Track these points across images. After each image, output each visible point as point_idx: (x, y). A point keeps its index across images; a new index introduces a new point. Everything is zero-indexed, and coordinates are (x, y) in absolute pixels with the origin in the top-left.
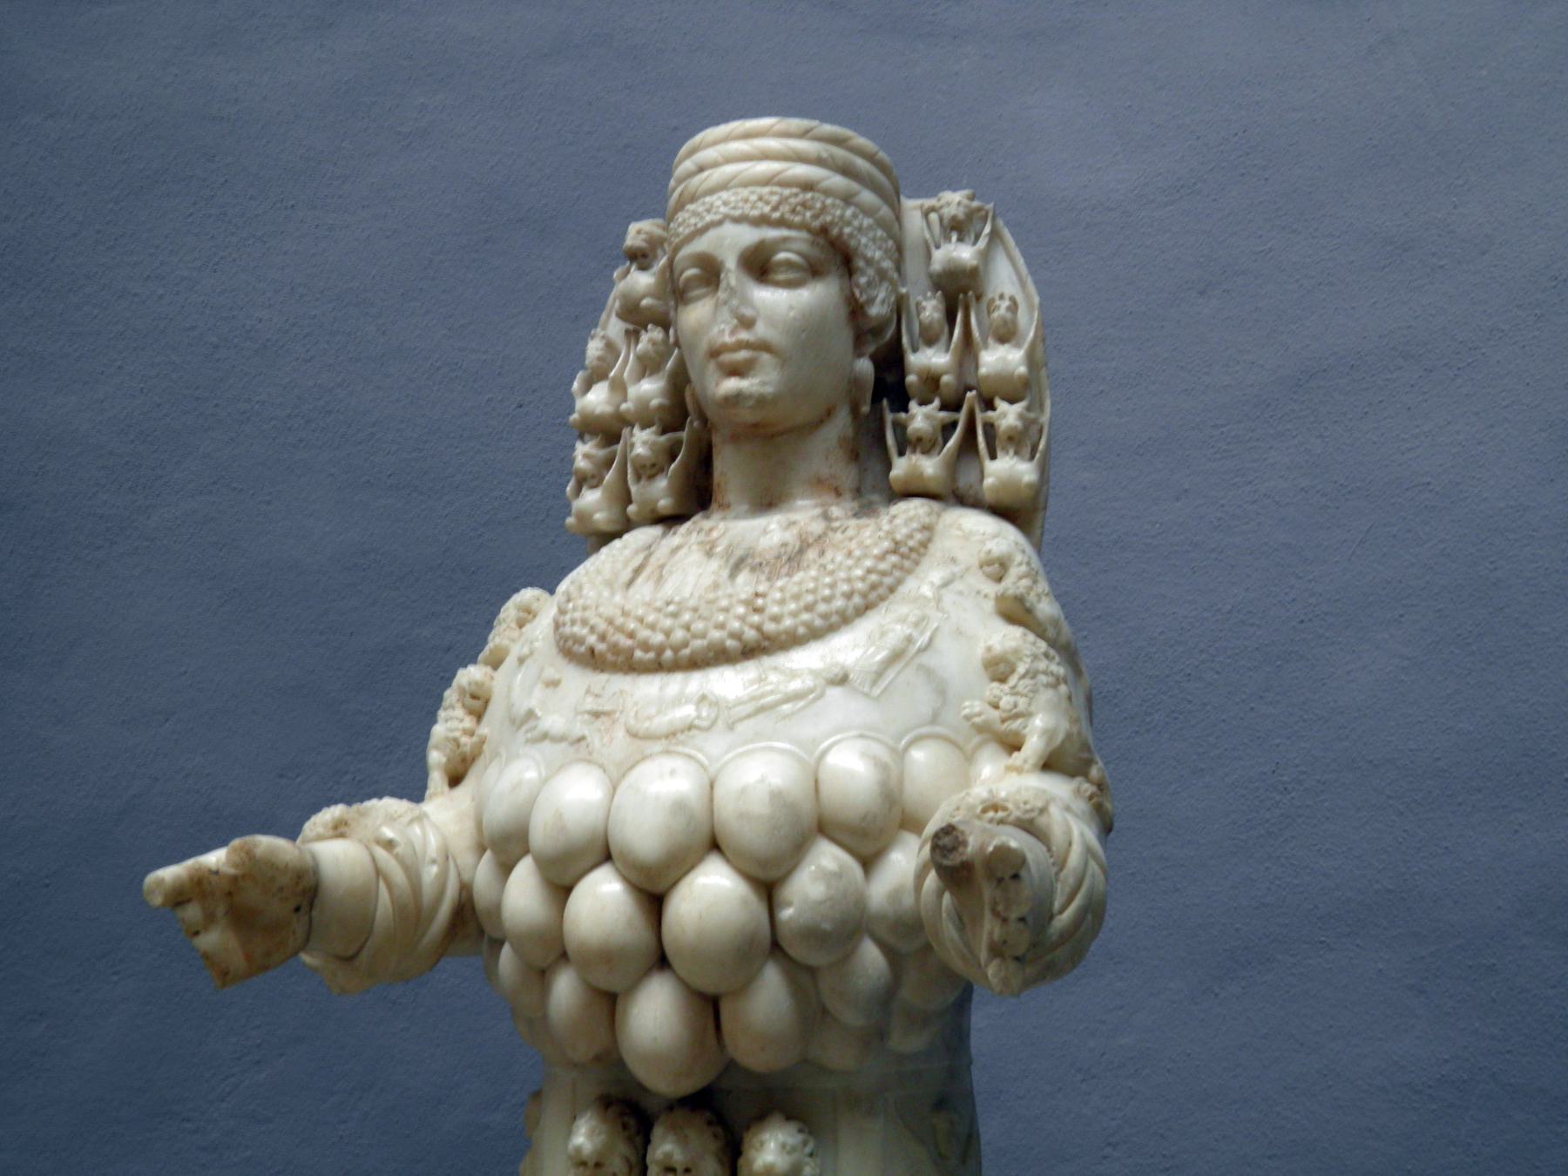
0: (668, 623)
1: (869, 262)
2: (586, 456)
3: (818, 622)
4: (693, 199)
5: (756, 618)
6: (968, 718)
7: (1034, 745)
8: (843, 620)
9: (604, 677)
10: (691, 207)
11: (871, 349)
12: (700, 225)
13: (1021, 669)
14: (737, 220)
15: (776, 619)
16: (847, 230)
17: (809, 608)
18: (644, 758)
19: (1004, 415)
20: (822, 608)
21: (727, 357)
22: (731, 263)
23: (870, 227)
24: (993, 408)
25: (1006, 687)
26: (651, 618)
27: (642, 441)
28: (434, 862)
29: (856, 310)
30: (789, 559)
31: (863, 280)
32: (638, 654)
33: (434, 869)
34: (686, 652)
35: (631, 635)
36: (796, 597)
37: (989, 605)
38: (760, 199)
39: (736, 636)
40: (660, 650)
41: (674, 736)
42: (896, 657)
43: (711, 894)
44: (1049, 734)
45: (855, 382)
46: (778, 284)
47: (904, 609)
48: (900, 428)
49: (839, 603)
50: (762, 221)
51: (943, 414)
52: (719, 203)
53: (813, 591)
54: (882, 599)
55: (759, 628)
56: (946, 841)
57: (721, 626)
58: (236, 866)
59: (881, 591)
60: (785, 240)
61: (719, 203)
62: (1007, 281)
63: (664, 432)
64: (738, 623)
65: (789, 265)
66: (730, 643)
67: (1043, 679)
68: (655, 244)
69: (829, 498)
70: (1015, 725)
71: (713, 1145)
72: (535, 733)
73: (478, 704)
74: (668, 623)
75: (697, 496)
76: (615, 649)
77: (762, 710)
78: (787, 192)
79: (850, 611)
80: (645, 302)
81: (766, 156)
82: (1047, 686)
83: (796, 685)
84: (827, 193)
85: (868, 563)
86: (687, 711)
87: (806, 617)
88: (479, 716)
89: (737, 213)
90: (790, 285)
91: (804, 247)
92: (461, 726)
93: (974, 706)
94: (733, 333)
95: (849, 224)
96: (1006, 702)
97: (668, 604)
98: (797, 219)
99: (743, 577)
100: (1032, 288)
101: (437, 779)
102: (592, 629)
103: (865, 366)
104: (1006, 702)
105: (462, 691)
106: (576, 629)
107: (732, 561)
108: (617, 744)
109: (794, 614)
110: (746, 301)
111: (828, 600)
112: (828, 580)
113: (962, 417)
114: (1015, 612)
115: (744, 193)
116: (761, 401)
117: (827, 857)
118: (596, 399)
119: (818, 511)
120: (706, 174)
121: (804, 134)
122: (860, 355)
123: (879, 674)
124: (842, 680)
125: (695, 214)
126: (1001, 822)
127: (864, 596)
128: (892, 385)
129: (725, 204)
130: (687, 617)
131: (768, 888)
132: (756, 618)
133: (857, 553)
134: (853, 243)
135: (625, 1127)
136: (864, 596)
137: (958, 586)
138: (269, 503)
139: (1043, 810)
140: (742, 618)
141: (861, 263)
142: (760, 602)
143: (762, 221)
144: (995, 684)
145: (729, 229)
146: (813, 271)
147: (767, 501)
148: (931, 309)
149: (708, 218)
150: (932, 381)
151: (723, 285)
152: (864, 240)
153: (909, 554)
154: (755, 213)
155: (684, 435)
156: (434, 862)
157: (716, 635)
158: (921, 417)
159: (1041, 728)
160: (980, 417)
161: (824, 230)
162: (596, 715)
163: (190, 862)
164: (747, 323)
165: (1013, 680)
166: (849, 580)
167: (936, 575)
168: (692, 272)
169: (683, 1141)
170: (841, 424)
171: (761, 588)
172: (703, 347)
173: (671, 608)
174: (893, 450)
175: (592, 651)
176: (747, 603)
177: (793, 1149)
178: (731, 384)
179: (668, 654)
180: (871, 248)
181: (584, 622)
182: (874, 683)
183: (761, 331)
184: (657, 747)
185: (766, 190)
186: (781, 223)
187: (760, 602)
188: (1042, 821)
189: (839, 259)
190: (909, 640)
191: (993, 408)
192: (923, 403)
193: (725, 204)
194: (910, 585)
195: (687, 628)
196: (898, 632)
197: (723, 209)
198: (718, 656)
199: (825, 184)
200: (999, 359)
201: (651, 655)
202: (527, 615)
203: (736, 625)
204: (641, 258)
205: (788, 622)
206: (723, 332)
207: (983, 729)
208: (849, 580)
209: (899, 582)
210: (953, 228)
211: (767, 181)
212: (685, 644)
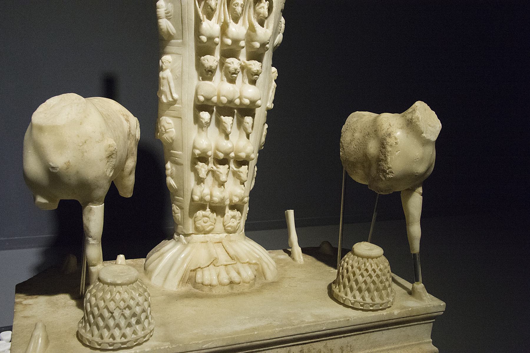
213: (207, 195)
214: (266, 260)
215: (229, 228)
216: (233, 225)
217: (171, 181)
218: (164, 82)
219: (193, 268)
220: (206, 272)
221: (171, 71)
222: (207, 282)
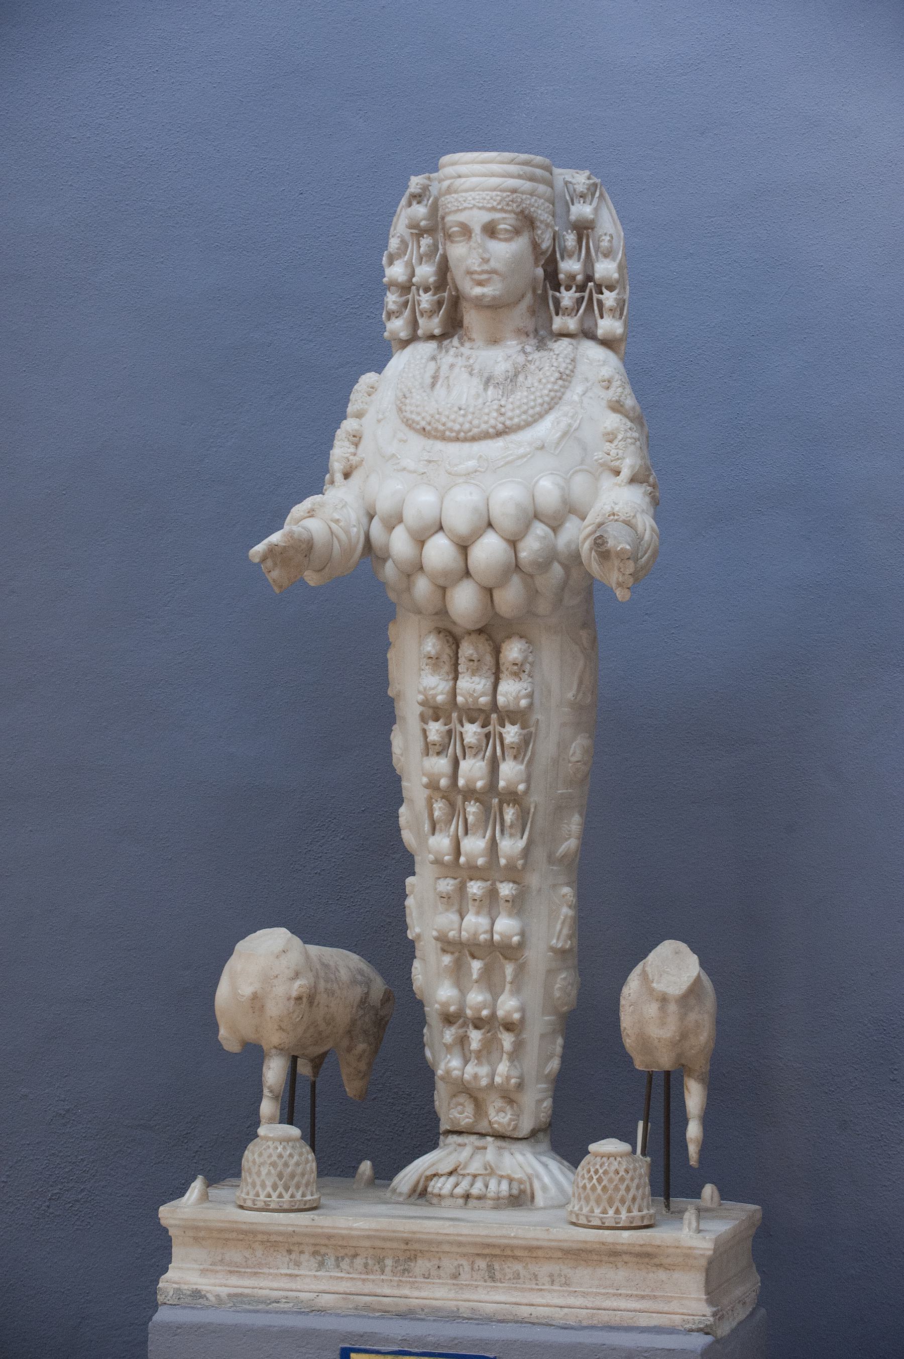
0: (461, 420)
1: (542, 222)
2: (394, 302)
3: (530, 419)
4: (456, 192)
5: (502, 419)
6: (596, 460)
7: (626, 473)
8: (541, 416)
9: (431, 442)
10: (455, 196)
11: (543, 262)
13: (620, 437)
14: (480, 208)
15: (511, 419)
16: (532, 209)
17: (525, 412)
20: (531, 412)
21: (476, 277)
22: (477, 229)
23: (543, 204)
24: (602, 294)
25: (613, 445)
26: (453, 417)
27: (426, 300)
28: (355, 526)
29: (535, 245)
30: (511, 381)
31: (539, 232)
32: (448, 433)
33: (355, 529)
34: (470, 434)
35: (444, 425)
36: (519, 407)
37: (604, 403)
38: (492, 198)
39: (494, 427)
40: (458, 432)
41: (469, 475)
42: (565, 434)
43: (489, 550)
44: (632, 467)
45: (535, 279)
46: (500, 240)
47: (566, 408)
48: (557, 302)
49: (538, 409)
50: (493, 209)
51: (578, 295)
52: (470, 198)
53: (526, 404)
54: (556, 404)
55: (503, 424)
56: (599, 541)
57: (486, 422)
58: (285, 542)
59: (556, 400)
60: (504, 218)
61: (471, 198)
62: (609, 226)
63: (434, 295)
64: (492, 421)
65: (506, 230)
66: (491, 430)
67: (629, 441)
68: (426, 188)
69: (524, 338)
70: (617, 463)
71: (488, 649)
73: (356, 439)
74: (461, 420)
75: (453, 326)
76: (436, 430)
77: (507, 463)
78: (505, 194)
79: (543, 412)
80: (423, 223)
81: (493, 175)
82: (631, 444)
83: (521, 451)
84: (523, 193)
85: (549, 386)
86: (472, 464)
87: (524, 417)
88: (356, 445)
89: (481, 205)
90: (506, 240)
91: (513, 222)
92: (349, 451)
93: (598, 455)
94: (479, 265)
95: (533, 206)
96: (613, 452)
97: (460, 409)
98: (510, 208)
99: (489, 393)
100: (620, 227)
101: (339, 477)
102: (423, 418)
103: (540, 272)
104: (613, 452)
105: (348, 433)
106: (413, 416)
107: (484, 380)
109: (519, 416)
110: (485, 250)
111: (533, 408)
112: (532, 397)
113: (586, 294)
114: (616, 407)
115: (484, 194)
116: (494, 298)
117: (540, 529)
118: (396, 271)
119: (519, 347)
120: (463, 180)
121: (511, 162)
122: (538, 266)
123: (558, 444)
124: (542, 447)
125: (457, 200)
126: (616, 520)
127: (549, 404)
128: (552, 278)
129: (474, 199)
130: (470, 417)
131: (513, 543)
132: (502, 419)
133: (544, 381)
134: (535, 215)
135: (448, 642)
136: (549, 404)
137: (589, 394)
138: (162, 263)
139: (634, 516)
140: (496, 419)
141: (538, 224)
142: (503, 410)
143: (493, 209)
144: (608, 444)
145: (475, 212)
146: (517, 232)
147: (494, 341)
148: (570, 239)
149: (465, 205)
150: (572, 277)
151: (474, 239)
152: (539, 212)
153: (566, 378)
154: (490, 206)
155: (446, 294)
156: (355, 526)
157: (484, 427)
158: (567, 297)
159: (629, 464)
160: (595, 296)
161: (522, 212)
162: (430, 462)
163: (266, 541)
164: (486, 261)
165: (616, 442)
166: (541, 396)
167: (579, 389)
169: (476, 649)
170: (528, 299)
171: (503, 403)
173: (462, 412)
174: (553, 312)
175: (424, 429)
176: (497, 410)
177: (525, 651)
178: (478, 291)
179: (462, 434)
180: (543, 215)
181: (418, 414)
182: (556, 448)
183: (493, 264)
185: (495, 193)
186: (502, 210)
187: (503, 410)
188: (633, 521)
189: (528, 223)
190: (570, 425)
191: (602, 294)
192: (568, 288)
193: (474, 199)
194: (568, 396)
195: (471, 423)
196: (565, 422)
197: (472, 202)
198: (486, 436)
199: (523, 188)
200: (605, 269)
201: (454, 434)
202: (372, 390)
203: (492, 422)
204: (418, 198)
205: (516, 420)
206: (474, 263)
207: (602, 465)
208: (541, 396)
209: (563, 394)
210: (581, 197)
211: (494, 189)
212: (470, 431)
213: (454, 1069)
214: (547, 1180)
215: (496, 1126)
216: (502, 1120)
217: (428, 1053)
218: (407, 911)
219: (429, 1173)
220: (443, 1179)
221: (415, 898)
222: (436, 1191)
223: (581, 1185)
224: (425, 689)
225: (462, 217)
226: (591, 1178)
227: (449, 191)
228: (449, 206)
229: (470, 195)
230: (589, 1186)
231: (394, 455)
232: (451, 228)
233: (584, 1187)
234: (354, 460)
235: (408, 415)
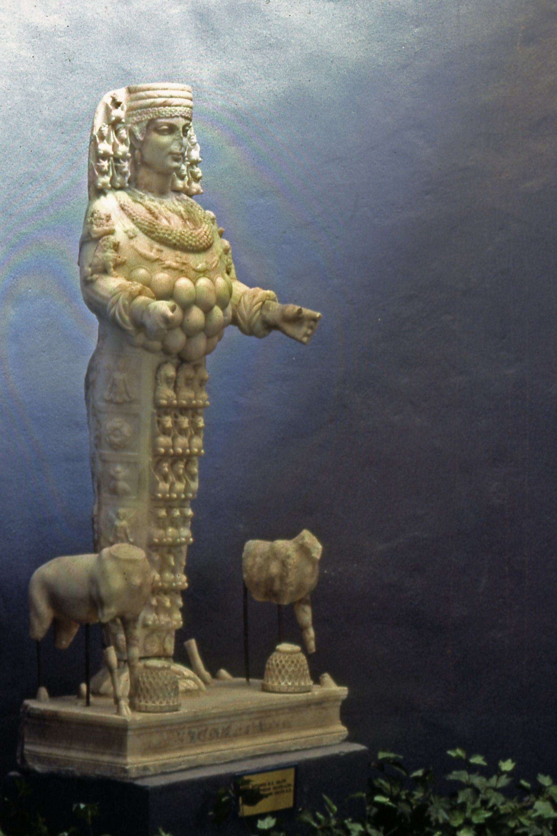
4: (170, 105)
10: (169, 108)
12: (173, 115)
14: (182, 116)
18: (199, 277)
19: (198, 172)
21: (175, 156)
32: (189, 247)
72: (165, 266)
108: (193, 273)
125: (171, 111)
145: (181, 119)
157: (204, 244)
168: (166, 127)
172: (168, 150)
184: (202, 275)
193: (180, 111)
201: (191, 248)
223: (290, 670)
224: (168, 397)
225: (173, 121)
226: (296, 666)
227: (164, 105)
228: (164, 113)
229: (178, 108)
230: (296, 670)
231: (157, 260)
232: (161, 126)
233: (293, 671)
234: (119, 260)
235: (161, 235)
